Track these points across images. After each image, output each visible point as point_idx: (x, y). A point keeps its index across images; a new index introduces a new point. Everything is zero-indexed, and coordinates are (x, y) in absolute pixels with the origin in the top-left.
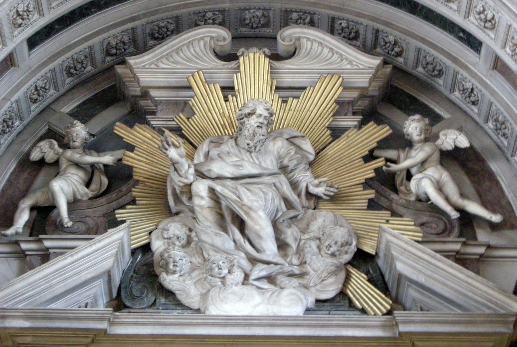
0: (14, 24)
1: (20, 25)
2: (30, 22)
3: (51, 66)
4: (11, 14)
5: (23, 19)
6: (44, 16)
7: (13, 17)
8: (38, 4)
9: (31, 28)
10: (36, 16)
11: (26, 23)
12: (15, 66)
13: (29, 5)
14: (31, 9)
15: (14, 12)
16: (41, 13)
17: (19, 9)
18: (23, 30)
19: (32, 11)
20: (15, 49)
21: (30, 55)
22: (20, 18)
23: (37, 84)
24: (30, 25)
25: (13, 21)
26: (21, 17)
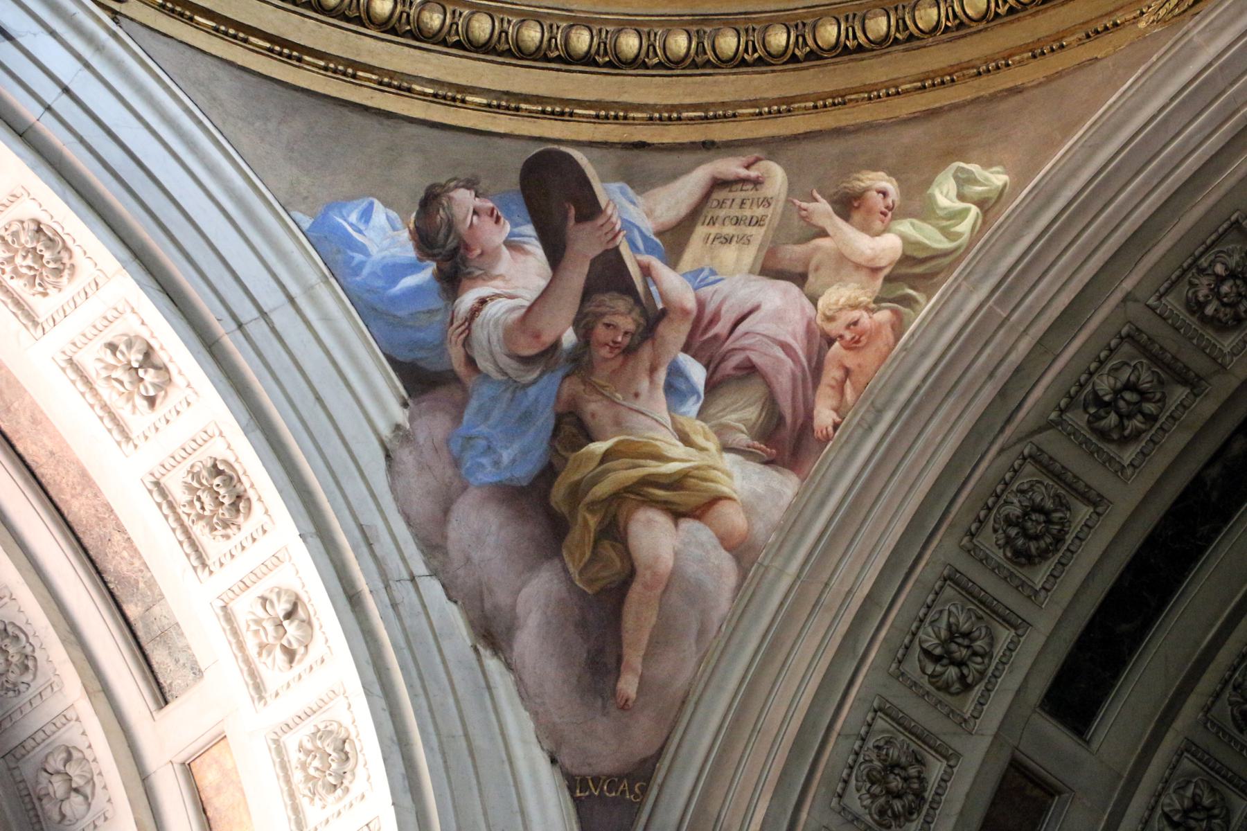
3: (1170, 742)
5: (960, 664)
7: (923, 671)
12: (1060, 793)
15: (920, 661)
17: (925, 646)
18: (989, 691)
23: (1167, 809)
24: (1000, 667)
26: (945, 661)
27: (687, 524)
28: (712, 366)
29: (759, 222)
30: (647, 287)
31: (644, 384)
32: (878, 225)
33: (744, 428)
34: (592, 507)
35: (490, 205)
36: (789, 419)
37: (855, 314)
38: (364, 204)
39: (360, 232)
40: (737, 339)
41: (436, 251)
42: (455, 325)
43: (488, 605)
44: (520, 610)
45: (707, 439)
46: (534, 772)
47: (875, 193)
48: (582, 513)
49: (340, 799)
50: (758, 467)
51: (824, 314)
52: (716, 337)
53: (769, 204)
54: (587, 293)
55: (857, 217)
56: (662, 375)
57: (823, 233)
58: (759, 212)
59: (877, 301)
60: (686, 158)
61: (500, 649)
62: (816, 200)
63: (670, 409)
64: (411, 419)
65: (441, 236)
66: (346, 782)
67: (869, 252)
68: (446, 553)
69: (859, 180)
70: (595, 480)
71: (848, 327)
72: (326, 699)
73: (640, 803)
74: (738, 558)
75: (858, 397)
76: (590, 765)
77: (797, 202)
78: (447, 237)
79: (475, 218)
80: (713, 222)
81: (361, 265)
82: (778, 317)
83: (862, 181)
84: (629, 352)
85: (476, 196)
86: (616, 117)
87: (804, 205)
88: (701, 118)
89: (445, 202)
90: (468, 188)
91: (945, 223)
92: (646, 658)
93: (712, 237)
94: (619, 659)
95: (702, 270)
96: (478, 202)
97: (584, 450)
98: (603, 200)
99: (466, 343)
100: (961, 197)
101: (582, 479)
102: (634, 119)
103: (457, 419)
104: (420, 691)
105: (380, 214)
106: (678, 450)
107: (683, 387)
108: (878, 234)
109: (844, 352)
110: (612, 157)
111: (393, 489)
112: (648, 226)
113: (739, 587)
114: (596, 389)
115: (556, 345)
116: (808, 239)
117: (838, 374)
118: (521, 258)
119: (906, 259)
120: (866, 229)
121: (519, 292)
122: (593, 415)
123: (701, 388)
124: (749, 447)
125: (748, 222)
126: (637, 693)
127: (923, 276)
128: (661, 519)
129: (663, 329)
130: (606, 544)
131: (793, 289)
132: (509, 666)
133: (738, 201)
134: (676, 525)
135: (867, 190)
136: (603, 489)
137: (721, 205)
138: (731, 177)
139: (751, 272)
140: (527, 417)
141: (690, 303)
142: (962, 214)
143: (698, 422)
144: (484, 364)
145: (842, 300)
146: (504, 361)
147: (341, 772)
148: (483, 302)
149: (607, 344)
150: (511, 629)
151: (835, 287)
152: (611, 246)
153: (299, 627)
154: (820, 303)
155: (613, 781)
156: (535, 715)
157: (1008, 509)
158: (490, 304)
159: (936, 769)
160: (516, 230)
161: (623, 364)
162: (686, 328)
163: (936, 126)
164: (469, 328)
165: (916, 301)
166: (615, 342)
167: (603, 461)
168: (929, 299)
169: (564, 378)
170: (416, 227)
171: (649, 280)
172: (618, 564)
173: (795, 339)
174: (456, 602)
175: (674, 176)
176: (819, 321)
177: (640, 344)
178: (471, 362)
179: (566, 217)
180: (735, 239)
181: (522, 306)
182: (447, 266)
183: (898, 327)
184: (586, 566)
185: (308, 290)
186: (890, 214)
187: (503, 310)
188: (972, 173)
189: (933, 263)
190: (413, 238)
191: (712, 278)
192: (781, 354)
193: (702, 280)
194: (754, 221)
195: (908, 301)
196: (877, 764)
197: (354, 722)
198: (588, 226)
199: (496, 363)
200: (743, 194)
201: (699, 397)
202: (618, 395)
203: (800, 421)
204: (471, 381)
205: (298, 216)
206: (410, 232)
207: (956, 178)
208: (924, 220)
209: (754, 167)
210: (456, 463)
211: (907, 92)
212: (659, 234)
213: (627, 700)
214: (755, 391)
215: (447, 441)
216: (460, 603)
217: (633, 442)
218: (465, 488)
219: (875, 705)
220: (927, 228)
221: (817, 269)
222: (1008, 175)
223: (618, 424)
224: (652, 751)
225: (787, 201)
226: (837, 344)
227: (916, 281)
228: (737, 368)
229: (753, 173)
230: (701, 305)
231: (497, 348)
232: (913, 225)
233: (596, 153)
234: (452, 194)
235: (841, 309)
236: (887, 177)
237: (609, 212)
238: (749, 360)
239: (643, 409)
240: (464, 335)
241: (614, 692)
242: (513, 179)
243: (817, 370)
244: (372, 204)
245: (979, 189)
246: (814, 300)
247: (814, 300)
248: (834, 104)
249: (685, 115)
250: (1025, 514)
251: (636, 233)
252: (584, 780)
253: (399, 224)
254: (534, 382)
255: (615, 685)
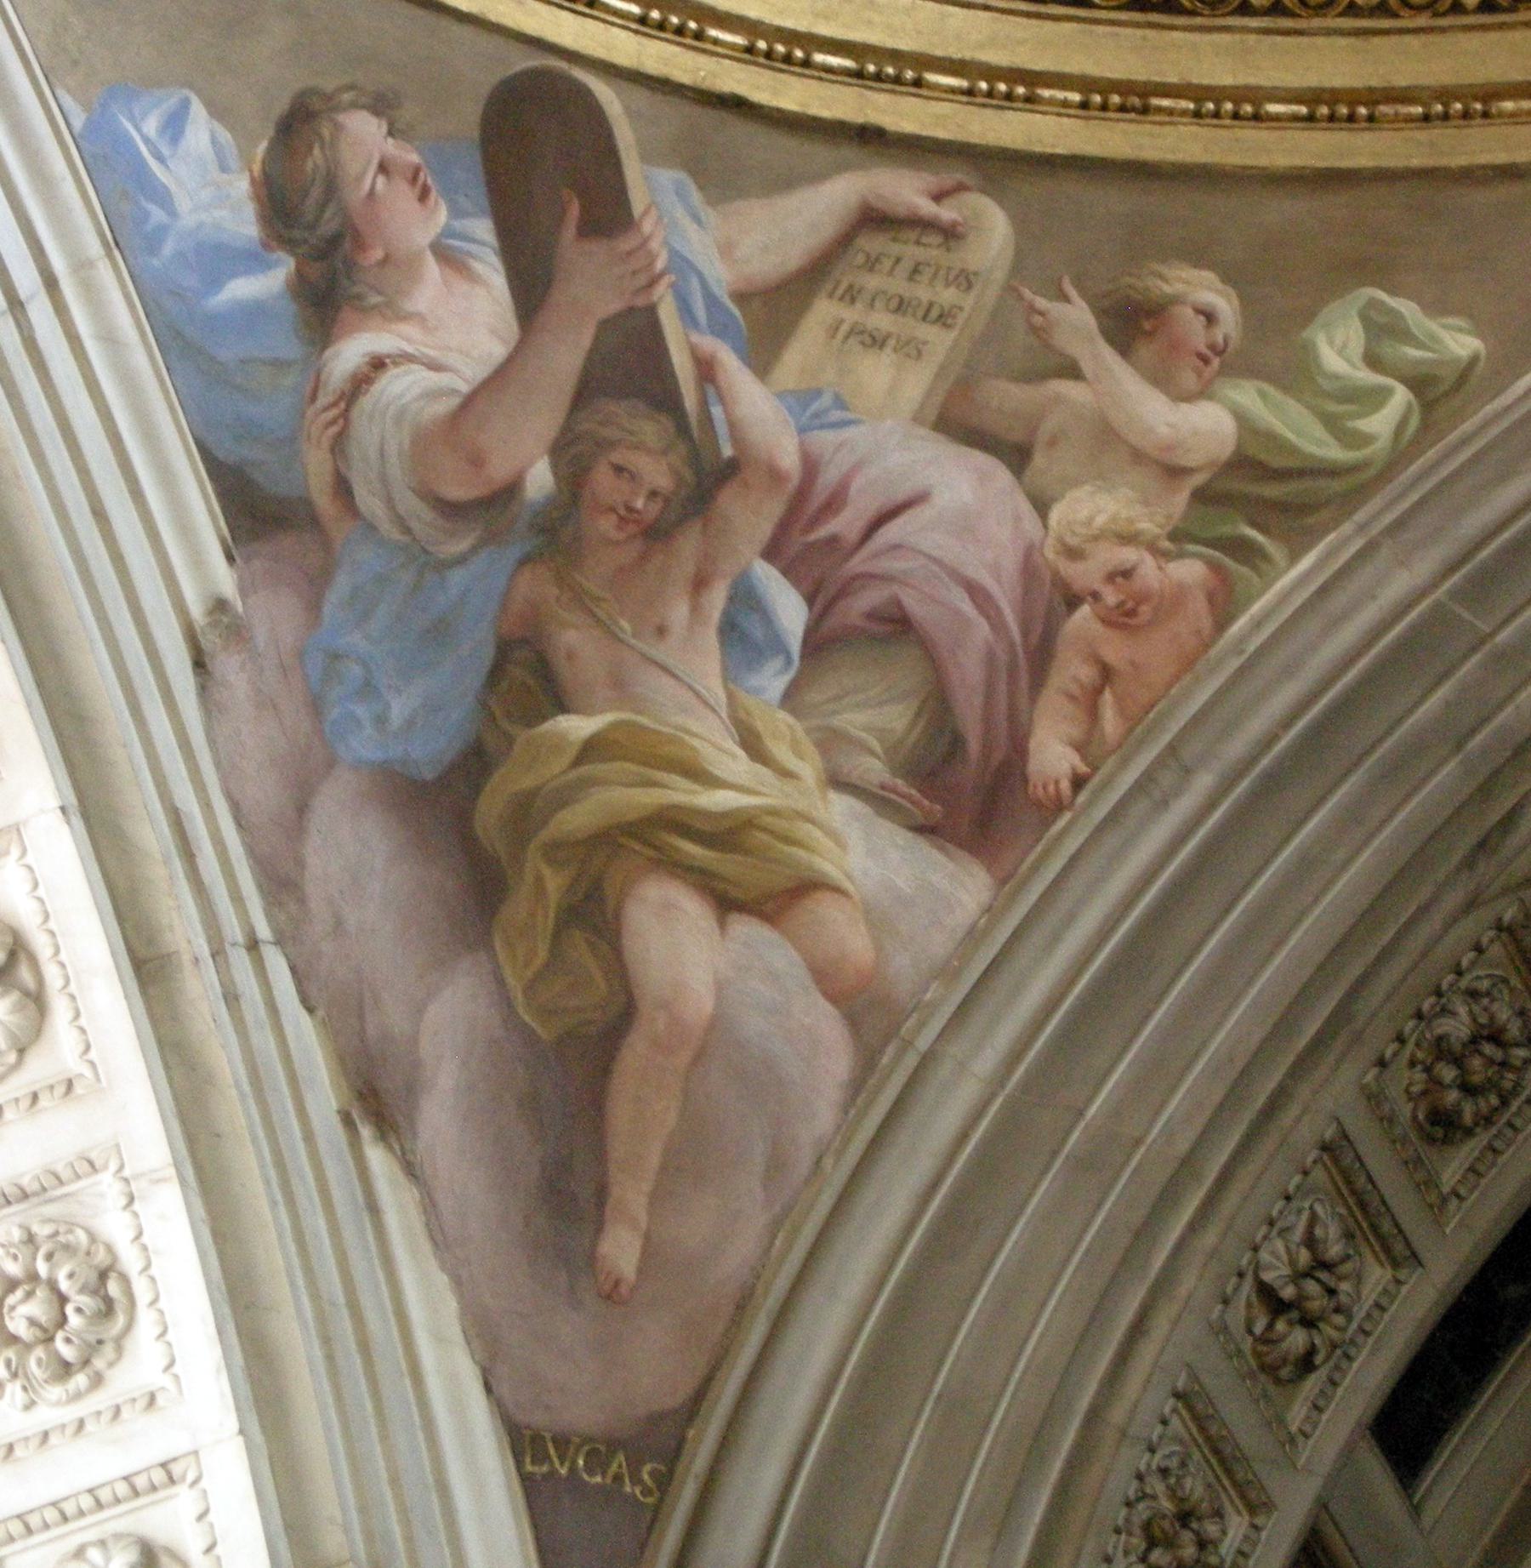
0: (1270, 1370)
1: (1306, 1363)
2: (1354, 1325)
4: (1236, 1316)
5: (1309, 1323)
6: (1420, 1264)
7: (1250, 1331)
8: (1363, 1206)
9: (1372, 1353)
10: (1377, 1275)
11: (1334, 1334)
13: (1318, 1232)
14: (1334, 1250)
15: (1249, 1305)
16: (1399, 1248)
17: (1268, 1277)
18: (1334, 1384)
19: (1347, 1258)
20: (1325, 1507)
21: (1416, 1511)
22: (1290, 1323)
25: (1257, 1355)
26: (1295, 1315)
27: (746, 928)
28: (820, 601)
29: (944, 319)
30: (704, 404)
31: (678, 612)
32: (1189, 380)
33: (878, 748)
34: (555, 852)
35: (415, 158)
36: (974, 745)
37: (1128, 555)
38: (172, 102)
39: (160, 159)
40: (876, 555)
41: (297, 234)
42: (322, 400)
43: (371, 1031)
44: (426, 1048)
45: (800, 756)
46: (459, 1410)
47: (1189, 312)
48: (534, 860)
49: (78, 1396)
50: (903, 837)
51: (1061, 540)
52: (833, 541)
53: (970, 286)
54: (585, 393)
55: (1145, 351)
56: (717, 598)
57: (1072, 371)
58: (948, 296)
59: (1174, 536)
60: (819, 152)
61: (394, 1127)
62: (1066, 299)
63: (725, 680)
64: (243, 591)
65: (310, 204)
66: (99, 1363)
67: (1163, 430)
68: (302, 901)
69: (1161, 277)
70: (564, 797)
71: (1111, 577)
72: (65, 1174)
73: (657, 1508)
74: (853, 1023)
75: (1130, 730)
76: (547, 1407)
77: (1027, 293)
78: (323, 206)
79: (381, 180)
80: (851, 295)
81: (163, 229)
82: (965, 526)
83: (1166, 281)
84: (656, 534)
85: (390, 133)
86: (680, 31)
87: (1041, 303)
88: (847, 72)
89: (326, 132)
90: (377, 112)
91: (1332, 407)
92: (657, 1198)
93: (845, 328)
94: (602, 1192)
95: (818, 393)
96: (391, 147)
97: (548, 726)
98: (638, 200)
99: (339, 446)
100: (1373, 361)
101: (539, 789)
102: (716, 42)
103: (314, 607)
104: (279, 1197)
105: (201, 131)
106: (734, 764)
107: (758, 633)
108: (1189, 398)
109: (1098, 628)
110: (676, 113)
111: (212, 741)
112: (720, 276)
113: (858, 1086)
114: (581, 600)
115: (511, 490)
116: (1035, 376)
117: (1087, 673)
118: (462, 286)
119: (1242, 463)
120: (1162, 380)
121: (452, 359)
122: (570, 656)
123: (795, 645)
124: (883, 787)
125: (920, 313)
126: (640, 1271)
127: (1282, 507)
128: (692, 908)
129: (729, 501)
130: (578, 936)
131: (1002, 475)
132: (410, 1169)
133: (907, 265)
134: (722, 924)
135: (1176, 300)
136: (578, 818)
137: (872, 264)
138: (901, 211)
139: (917, 419)
140: (439, 633)
141: (789, 459)
142: (1374, 398)
143: (782, 715)
144: (368, 500)
145: (1100, 520)
146: (410, 504)
147: (92, 1338)
148: (378, 364)
149: (613, 509)
150: (412, 1090)
151: (1087, 488)
152: (640, 302)
153: (18, 1009)
154: (1055, 515)
155: (600, 1451)
156: (458, 1282)
157: (1445, 1026)
158: (392, 372)
159: (1237, 1525)
160: (458, 225)
161: (644, 557)
162: (775, 509)
163: (1336, 205)
164: (345, 415)
165: (1266, 557)
166: (630, 509)
167: (578, 761)
168: (1294, 558)
169: (524, 562)
170: (264, 172)
171: (711, 391)
172: (603, 985)
173: (999, 582)
174: (310, 1010)
175: (785, 182)
176: (1050, 554)
177: (683, 520)
178: (343, 489)
179: (560, 220)
180: (892, 342)
181: (454, 392)
182: (315, 271)
183: (1224, 606)
184: (539, 977)
185: (81, 266)
186: (1216, 362)
187: (416, 391)
188: (1398, 315)
189: (1307, 484)
190: (257, 198)
191: (837, 415)
192: (967, 607)
193: (816, 415)
194: (934, 313)
195: (1241, 549)
196: (1167, 1505)
197: (140, 1235)
198: (598, 249)
199: (390, 502)
200: (920, 253)
201: (789, 661)
202: (625, 624)
203: (998, 757)
204: (340, 530)
205: (68, 101)
206: (253, 181)
207: (1365, 319)
208: (1286, 389)
209: (947, 202)
210: (316, 706)
211: (1277, 118)
212: (741, 298)
213: (617, 1284)
214: (906, 672)
215: (300, 654)
216: (321, 1013)
217: (644, 728)
218: (331, 763)
219: (1180, 1385)
220: (1293, 407)
221: (1053, 442)
222: (1483, 339)
223: (621, 688)
224: (677, 1396)
225: (1010, 289)
226: (1085, 610)
227: (1266, 513)
228: (871, 615)
229: (946, 213)
230: (811, 466)
231: (395, 470)
232: (1263, 395)
233: (640, 96)
234: (341, 118)
235: (1096, 538)
236: (1220, 285)
237: (647, 227)
238: (899, 604)
239: (670, 662)
240: (334, 429)
241: (592, 1258)
242: (468, 116)
243: (1041, 655)
244: (185, 105)
245: (1413, 353)
246: (1042, 507)
247: (1042, 507)
248: (1122, 109)
249: (819, 58)
250: (1474, 1040)
251: (695, 283)
252: (537, 1439)
253: (233, 162)
254: (461, 560)
255: (594, 1245)
